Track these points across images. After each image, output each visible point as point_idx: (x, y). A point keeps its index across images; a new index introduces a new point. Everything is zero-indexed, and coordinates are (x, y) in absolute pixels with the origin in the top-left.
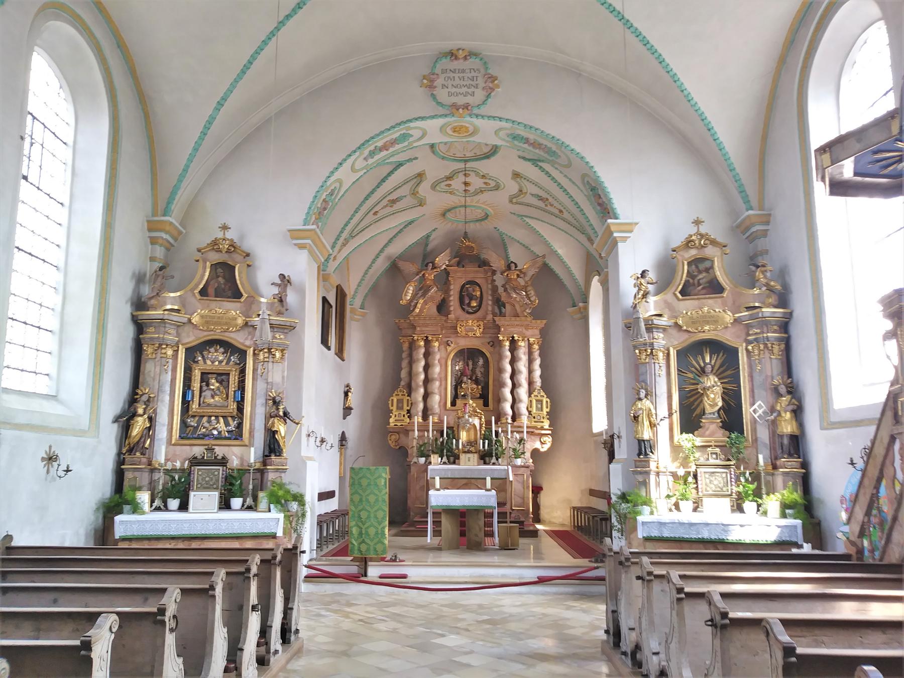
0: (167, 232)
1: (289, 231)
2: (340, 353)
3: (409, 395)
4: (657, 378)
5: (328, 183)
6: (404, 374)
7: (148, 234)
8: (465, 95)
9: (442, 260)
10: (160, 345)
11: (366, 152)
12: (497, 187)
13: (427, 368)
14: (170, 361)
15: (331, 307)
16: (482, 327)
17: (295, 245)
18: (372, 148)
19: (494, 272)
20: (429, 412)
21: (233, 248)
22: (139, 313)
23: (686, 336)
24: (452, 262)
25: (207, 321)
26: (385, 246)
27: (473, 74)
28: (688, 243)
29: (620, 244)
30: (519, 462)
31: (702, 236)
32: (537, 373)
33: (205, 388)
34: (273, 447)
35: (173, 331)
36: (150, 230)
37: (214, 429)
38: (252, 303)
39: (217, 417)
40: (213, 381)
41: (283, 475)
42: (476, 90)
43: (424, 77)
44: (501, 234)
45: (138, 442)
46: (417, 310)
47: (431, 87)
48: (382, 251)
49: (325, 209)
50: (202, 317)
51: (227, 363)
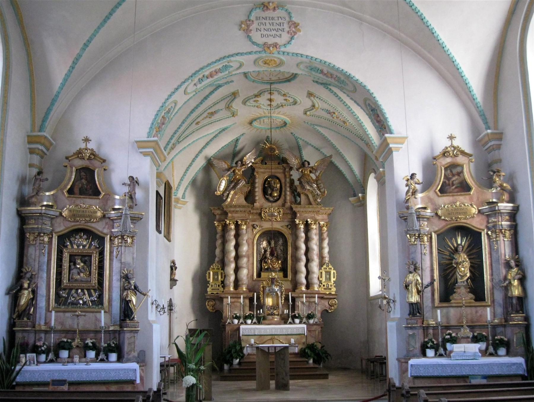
0: (42, 144)
1: (137, 142)
2: (168, 237)
3: (223, 268)
4: (423, 257)
5: (167, 104)
6: (218, 251)
7: (28, 146)
8: (274, 36)
9: (250, 159)
10: (39, 233)
11: (196, 80)
12: (295, 103)
13: (237, 246)
14: (47, 246)
15: (162, 198)
16: (282, 213)
17: (141, 153)
18: (201, 76)
19: (291, 169)
20: (240, 283)
21: (94, 155)
22: (23, 208)
23: (444, 223)
24: (257, 160)
25: (74, 215)
26: (204, 148)
27: (280, 21)
28: (444, 154)
29: (394, 153)
30: (311, 321)
31: (455, 148)
32: (326, 250)
33: (72, 267)
34: (127, 312)
35: (49, 223)
36: (29, 143)
37: (81, 299)
38: (108, 200)
39: (82, 290)
40: (79, 261)
41: (136, 335)
42: (283, 34)
43: (242, 23)
44: (296, 138)
45: (25, 310)
46: (229, 200)
47: (247, 31)
48: (200, 151)
49: (163, 124)
50: (70, 211)
51: (89, 247)
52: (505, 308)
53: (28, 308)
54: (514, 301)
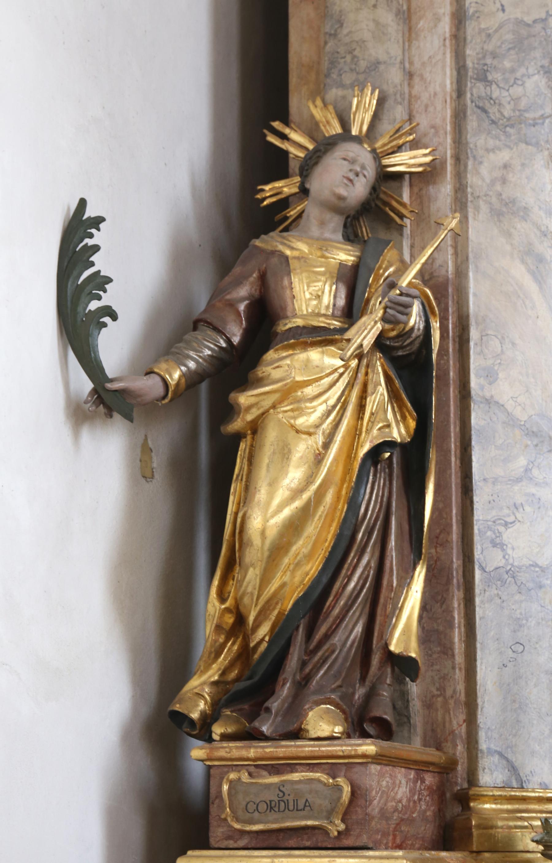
45: (315, 603)
53: (354, 581)
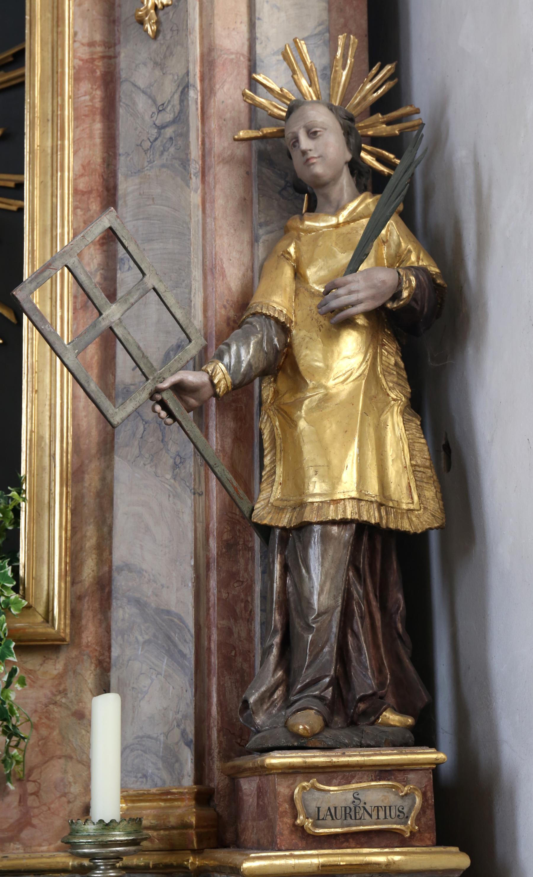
52: (221, 662)
54: (321, 577)
